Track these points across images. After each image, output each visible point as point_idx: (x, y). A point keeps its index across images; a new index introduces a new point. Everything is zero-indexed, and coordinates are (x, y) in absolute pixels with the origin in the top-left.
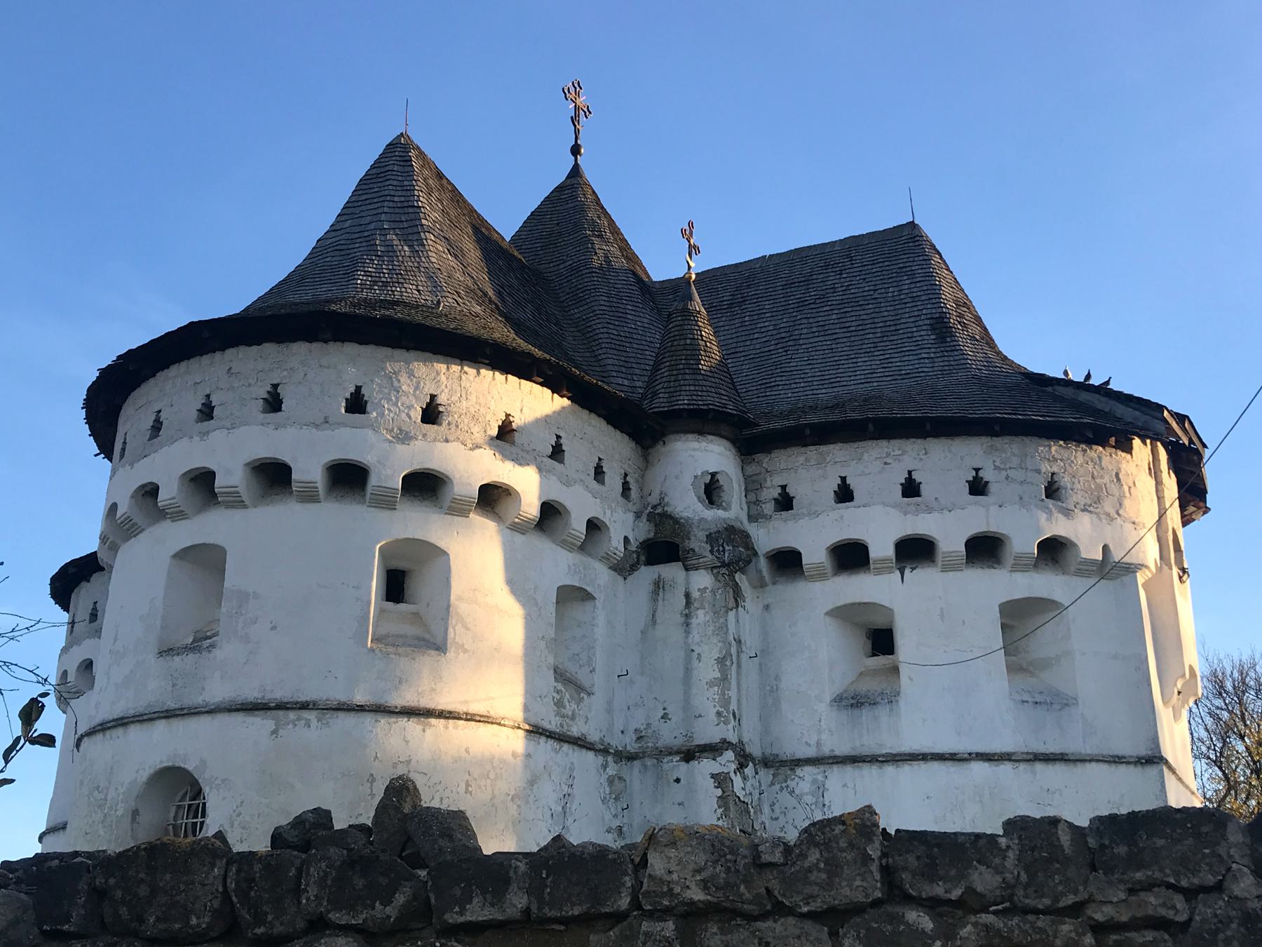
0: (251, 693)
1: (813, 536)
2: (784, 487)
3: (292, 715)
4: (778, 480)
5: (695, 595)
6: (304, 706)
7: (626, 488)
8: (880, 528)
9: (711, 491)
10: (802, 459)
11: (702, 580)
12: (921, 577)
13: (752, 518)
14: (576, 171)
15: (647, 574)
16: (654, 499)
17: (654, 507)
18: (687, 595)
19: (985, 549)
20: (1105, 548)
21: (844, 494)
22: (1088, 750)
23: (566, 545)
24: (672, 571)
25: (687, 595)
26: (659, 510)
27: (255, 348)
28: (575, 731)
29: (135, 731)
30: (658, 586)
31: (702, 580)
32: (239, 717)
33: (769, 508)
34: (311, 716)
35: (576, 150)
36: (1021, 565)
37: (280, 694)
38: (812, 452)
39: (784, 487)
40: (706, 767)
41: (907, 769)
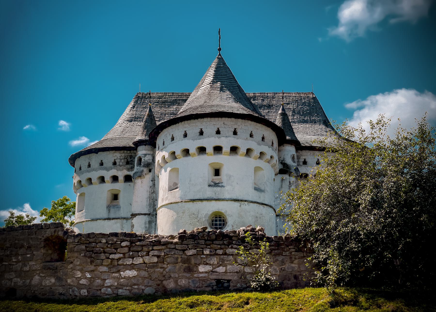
0: (235, 197)
2: (305, 159)
3: (243, 203)
4: (304, 157)
5: (291, 182)
6: (246, 201)
10: (309, 153)
11: (293, 179)
16: (282, 159)
17: (282, 161)
18: (290, 182)
21: (318, 163)
24: (286, 176)
25: (290, 182)
26: (283, 162)
27: (230, 119)
29: (205, 203)
30: (282, 180)
31: (293, 179)
32: (233, 202)
33: (301, 163)
34: (246, 203)
39: (305, 159)
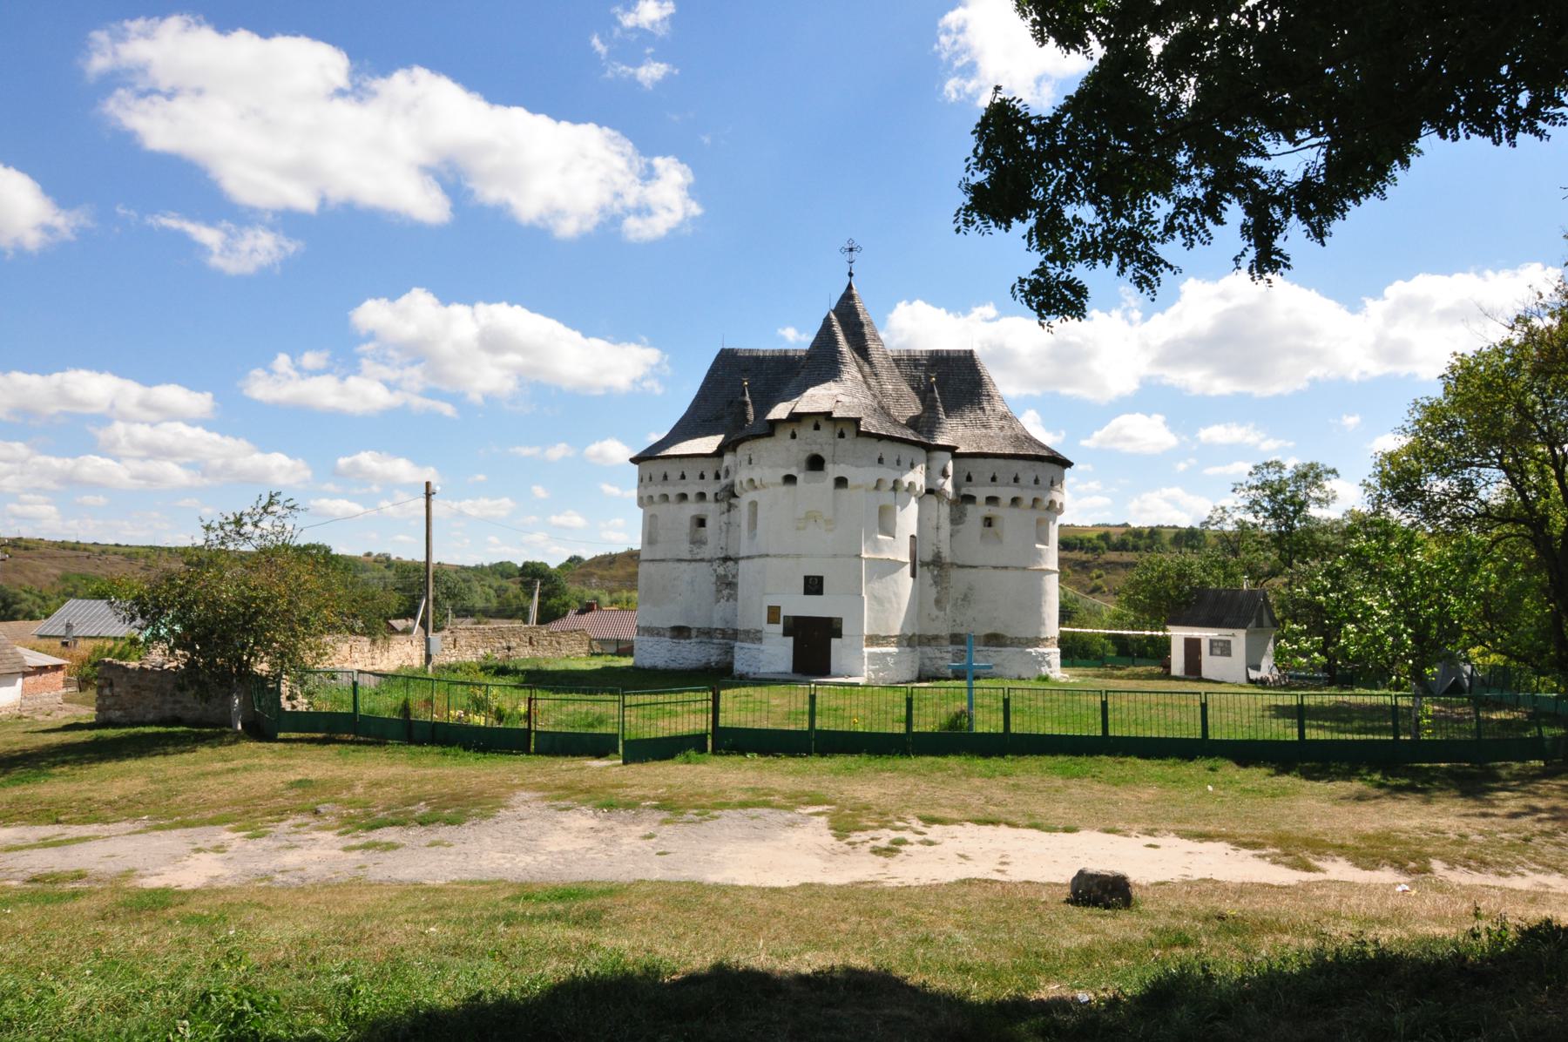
7: (717, 477)
14: (850, 287)
35: (851, 275)
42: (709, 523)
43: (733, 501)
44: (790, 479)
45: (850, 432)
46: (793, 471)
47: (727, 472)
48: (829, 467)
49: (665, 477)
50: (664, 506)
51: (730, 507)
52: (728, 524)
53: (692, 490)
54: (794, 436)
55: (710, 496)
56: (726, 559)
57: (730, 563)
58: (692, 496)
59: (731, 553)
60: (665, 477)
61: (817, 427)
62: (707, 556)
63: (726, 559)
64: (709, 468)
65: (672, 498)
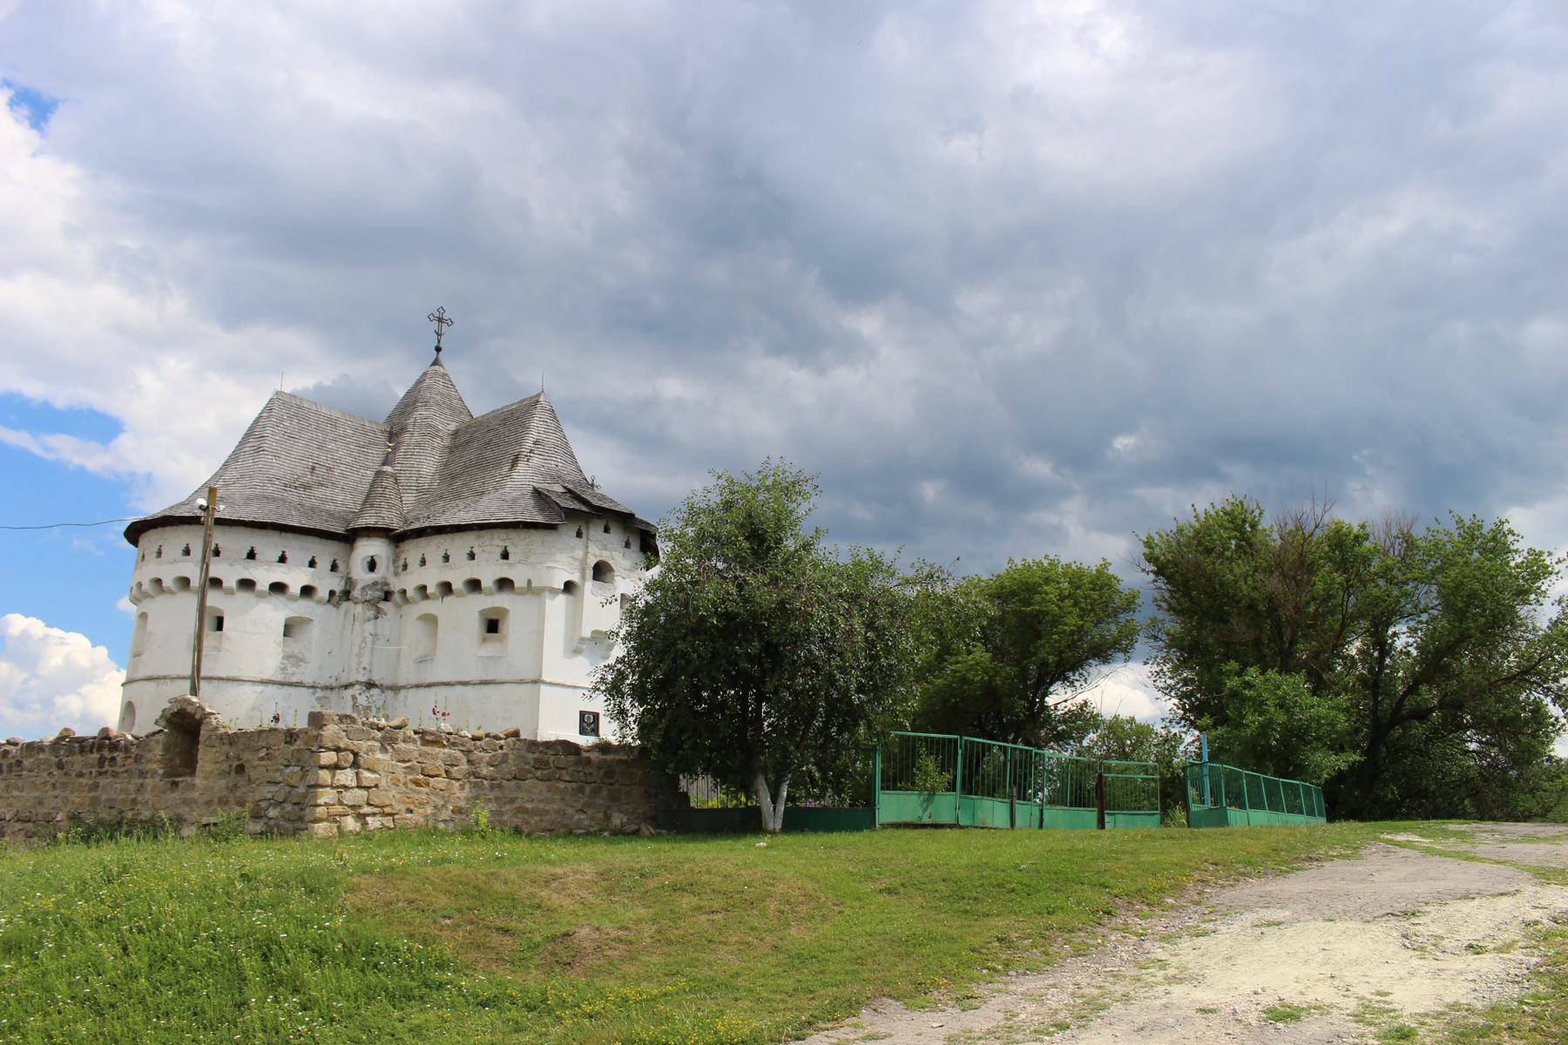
0: (150, 674)
1: (409, 582)
6: (165, 678)
7: (334, 568)
8: (432, 580)
9: (372, 565)
12: (449, 599)
13: (396, 574)
15: (345, 605)
19: (474, 585)
20: (529, 582)
22: (507, 678)
23: (293, 599)
28: (294, 679)
30: (347, 612)
35: (438, 349)
36: (490, 593)
37: (161, 673)
38: (415, 541)
40: (350, 691)
41: (433, 689)
42: (315, 631)
43: (382, 605)
44: (569, 587)
45: (635, 546)
46: (575, 578)
47: (372, 565)
48: (618, 580)
49: (251, 555)
50: (244, 596)
51: (378, 613)
52: (375, 636)
53: (296, 578)
54: (579, 535)
55: (323, 593)
56: (370, 685)
57: (375, 691)
58: (295, 589)
59: (376, 678)
60: (251, 555)
61: (607, 530)
62: (308, 680)
63: (370, 685)
64: (326, 552)
65: (263, 584)
